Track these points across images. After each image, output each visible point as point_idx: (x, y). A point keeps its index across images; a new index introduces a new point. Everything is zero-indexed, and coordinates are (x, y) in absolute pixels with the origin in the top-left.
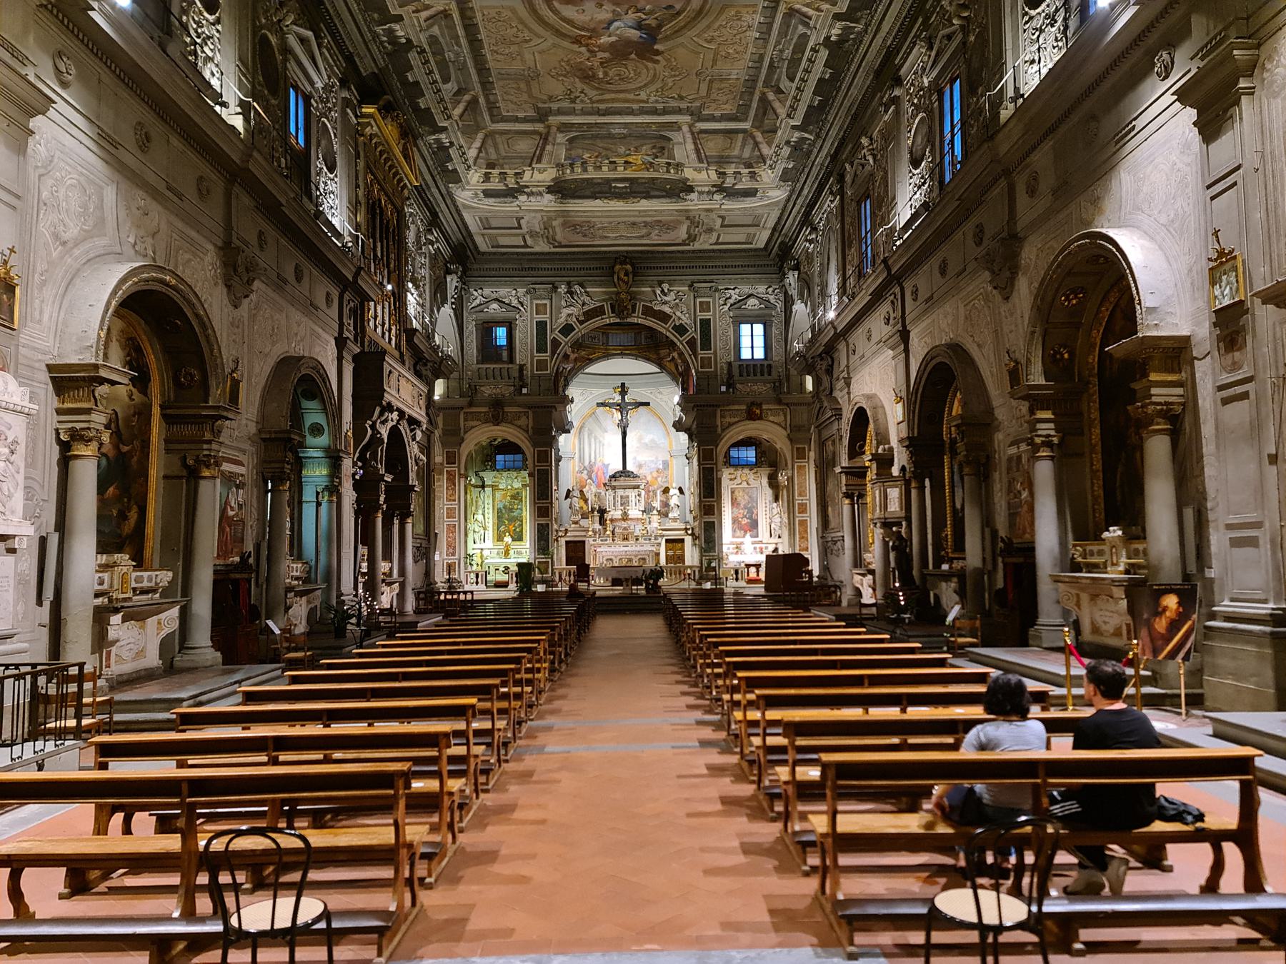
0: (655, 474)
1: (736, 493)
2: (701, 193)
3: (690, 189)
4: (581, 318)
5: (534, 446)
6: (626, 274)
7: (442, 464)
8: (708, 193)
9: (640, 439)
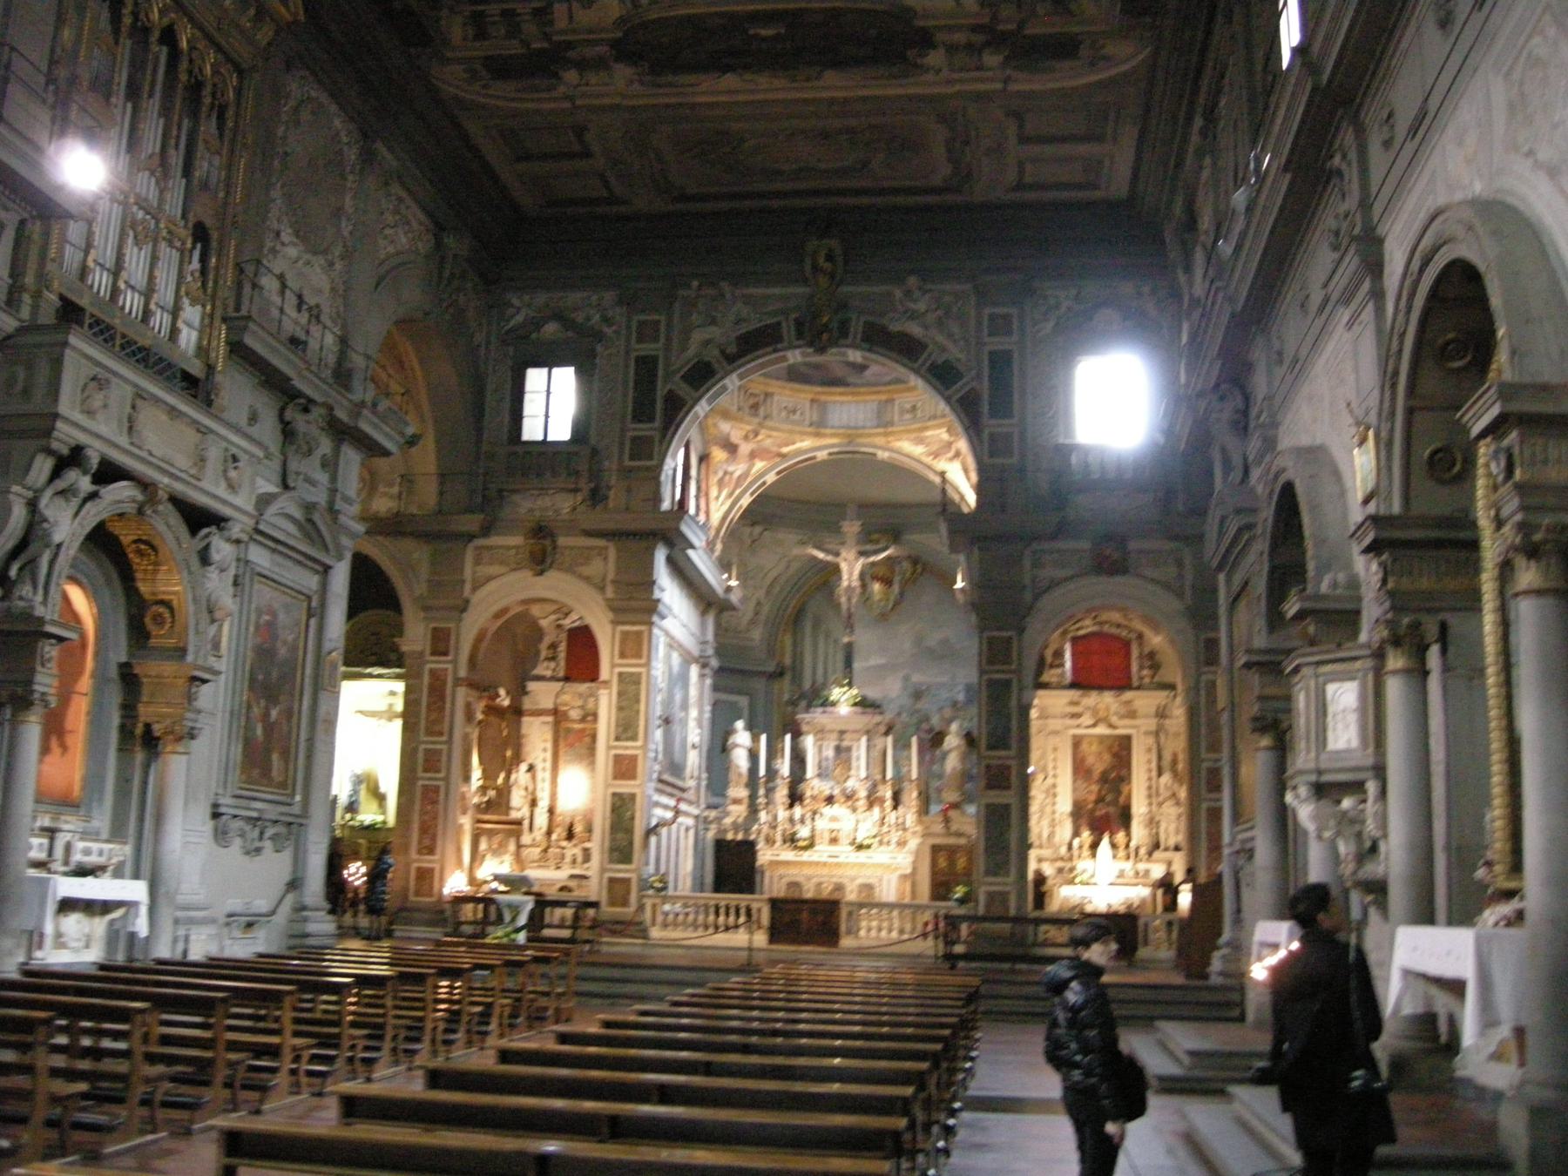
0: (948, 713)
1: (1084, 746)
2: (952, 49)
3: (925, 40)
4: (732, 349)
5: (615, 623)
6: (830, 258)
7: (421, 654)
8: (970, 46)
9: (919, 640)
